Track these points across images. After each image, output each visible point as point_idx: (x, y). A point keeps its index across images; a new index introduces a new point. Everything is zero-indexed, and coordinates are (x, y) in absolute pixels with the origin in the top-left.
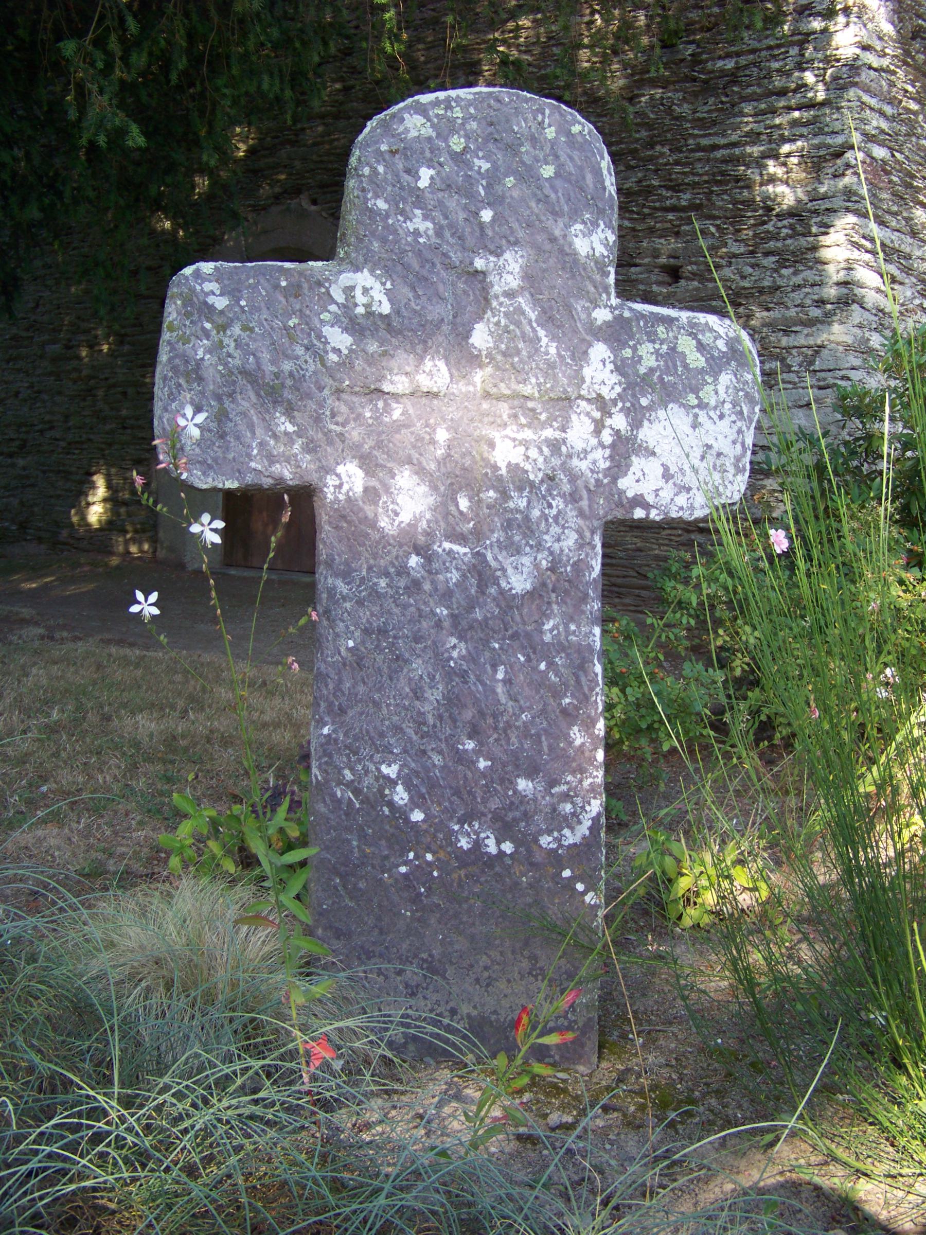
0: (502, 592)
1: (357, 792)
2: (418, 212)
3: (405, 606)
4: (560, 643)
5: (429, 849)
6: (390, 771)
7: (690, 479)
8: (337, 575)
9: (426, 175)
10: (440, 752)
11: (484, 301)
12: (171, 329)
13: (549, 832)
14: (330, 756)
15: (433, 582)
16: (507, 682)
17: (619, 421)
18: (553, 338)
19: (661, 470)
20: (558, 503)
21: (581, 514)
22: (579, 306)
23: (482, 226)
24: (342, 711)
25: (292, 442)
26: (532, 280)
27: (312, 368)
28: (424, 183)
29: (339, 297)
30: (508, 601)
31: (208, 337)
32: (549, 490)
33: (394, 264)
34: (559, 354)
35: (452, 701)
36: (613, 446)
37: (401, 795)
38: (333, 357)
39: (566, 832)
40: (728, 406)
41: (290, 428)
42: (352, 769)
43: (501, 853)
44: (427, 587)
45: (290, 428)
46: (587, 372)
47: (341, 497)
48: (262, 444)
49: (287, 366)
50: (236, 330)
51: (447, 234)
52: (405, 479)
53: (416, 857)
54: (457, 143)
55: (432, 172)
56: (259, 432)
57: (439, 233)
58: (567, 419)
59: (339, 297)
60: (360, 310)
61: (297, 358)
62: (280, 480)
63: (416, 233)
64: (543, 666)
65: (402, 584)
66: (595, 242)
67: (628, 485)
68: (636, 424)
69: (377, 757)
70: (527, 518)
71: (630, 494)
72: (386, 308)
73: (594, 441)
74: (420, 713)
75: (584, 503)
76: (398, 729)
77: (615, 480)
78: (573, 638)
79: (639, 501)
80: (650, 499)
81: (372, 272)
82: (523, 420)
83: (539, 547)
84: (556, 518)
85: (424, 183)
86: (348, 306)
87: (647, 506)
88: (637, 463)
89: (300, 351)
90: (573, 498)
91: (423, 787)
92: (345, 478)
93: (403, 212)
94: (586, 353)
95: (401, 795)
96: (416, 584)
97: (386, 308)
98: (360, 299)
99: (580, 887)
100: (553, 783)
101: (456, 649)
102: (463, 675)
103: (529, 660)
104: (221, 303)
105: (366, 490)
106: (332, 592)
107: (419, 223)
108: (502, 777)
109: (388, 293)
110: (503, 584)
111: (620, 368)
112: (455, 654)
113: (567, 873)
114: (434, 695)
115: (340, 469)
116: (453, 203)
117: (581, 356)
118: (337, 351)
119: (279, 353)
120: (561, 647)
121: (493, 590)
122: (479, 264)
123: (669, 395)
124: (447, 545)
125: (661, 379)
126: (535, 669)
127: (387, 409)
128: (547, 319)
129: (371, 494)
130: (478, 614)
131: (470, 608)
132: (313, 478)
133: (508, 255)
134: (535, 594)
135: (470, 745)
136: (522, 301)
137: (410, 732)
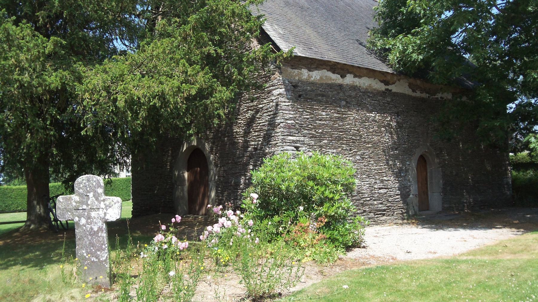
6: (84, 252)
9: (81, 185)
11: (89, 198)
17: (105, 210)
26: (94, 196)
30: (94, 232)
33: (80, 195)
35: (90, 243)
37: (85, 254)
52: (82, 218)
54: (84, 181)
66: (100, 191)
67: (106, 218)
88: (107, 215)
90: (101, 219)
91: (88, 253)
95: (85, 254)
96: (84, 231)
101: (90, 237)
104: (61, 201)
107: (81, 191)
108: (96, 252)
111: (105, 204)
114: (88, 243)
116: (85, 188)
117: (100, 203)
119: (68, 206)
120: (101, 236)
123: (110, 207)
128: (96, 200)
129: (79, 221)
134: (98, 231)
136: (93, 198)
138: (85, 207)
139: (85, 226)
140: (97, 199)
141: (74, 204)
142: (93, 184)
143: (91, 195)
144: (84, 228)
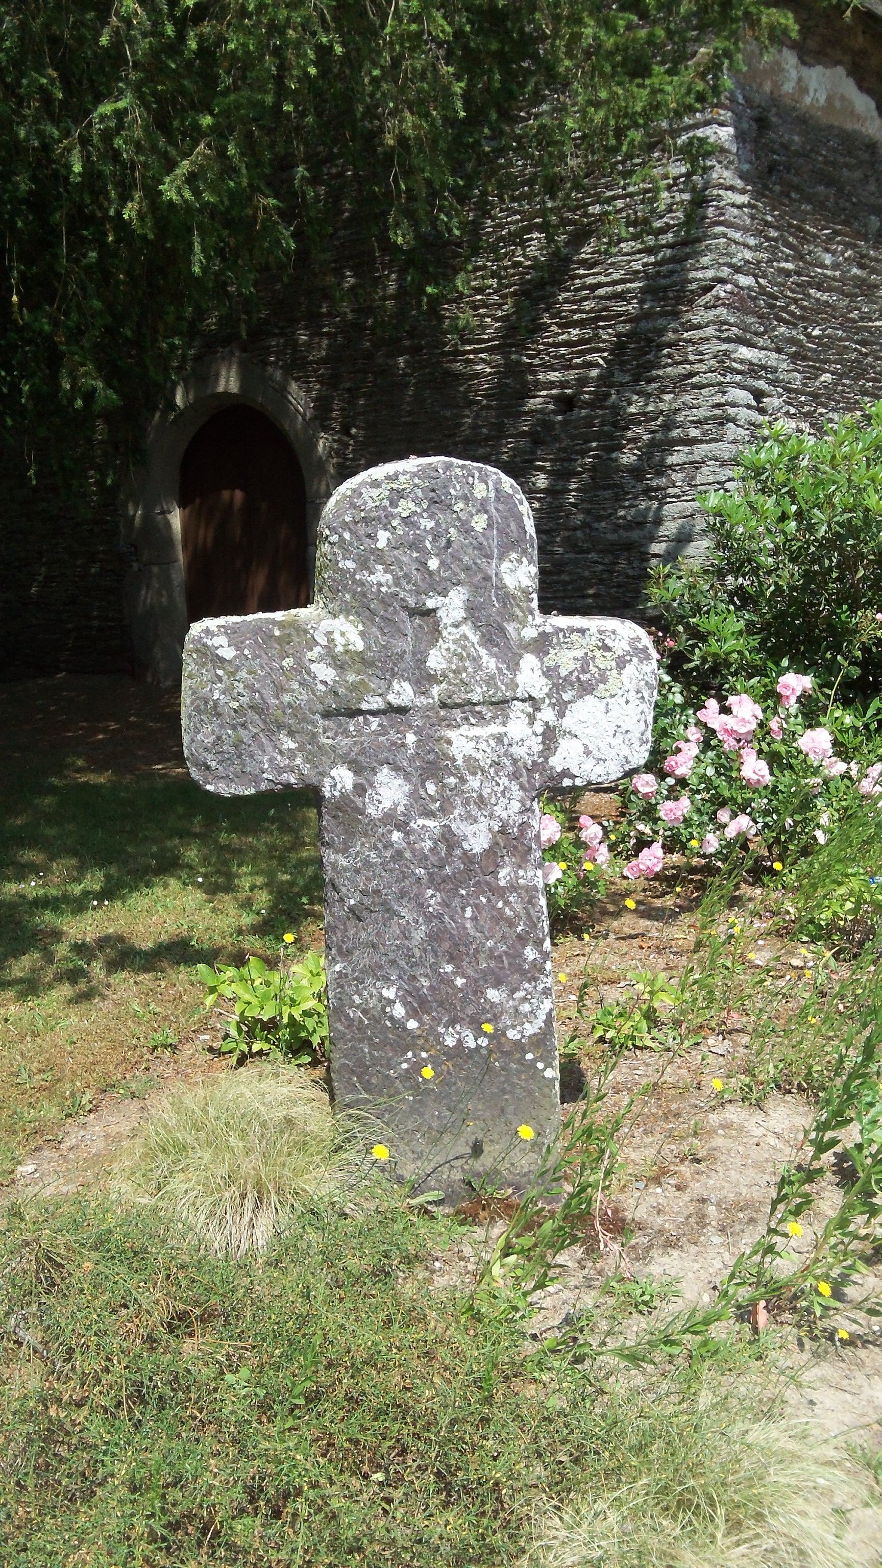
0: (465, 853)
1: (365, 1012)
2: (380, 567)
3: (391, 871)
4: (512, 886)
5: (423, 1049)
6: (390, 993)
7: (606, 753)
8: (337, 852)
9: (383, 538)
10: (427, 976)
11: (436, 633)
12: (190, 677)
13: (514, 1027)
14: (342, 987)
15: (413, 851)
16: (474, 919)
17: (547, 714)
18: (492, 655)
19: (582, 749)
20: (504, 781)
21: (522, 787)
22: (510, 628)
23: (431, 573)
24: (349, 952)
25: (295, 756)
26: (473, 611)
27: (305, 697)
28: (382, 544)
29: (323, 641)
30: (468, 858)
31: (221, 681)
32: (496, 772)
33: (364, 606)
34: (498, 668)
35: (433, 938)
36: (543, 734)
37: (399, 1011)
38: (322, 687)
39: (527, 1025)
40: (632, 693)
41: (293, 745)
42: (360, 995)
43: (479, 1047)
44: (408, 855)
45: (293, 745)
46: (520, 679)
47: (337, 794)
48: (271, 760)
49: (287, 698)
50: (243, 674)
51: (404, 582)
52: (384, 775)
53: (414, 1056)
54: (406, 507)
55: (388, 534)
56: (269, 749)
57: (397, 584)
58: (507, 717)
59: (323, 641)
60: (339, 649)
61: (293, 691)
62: (288, 786)
63: (380, 584)
64: (500, 905)
65: (388, 854)
66: (521, 574)
67: (557, 762)
68: (561, 715)
69: (379, 984)
70: (481, 796)
71: (559, 769)
72: (360, 646)
73: (530, 731)
74: (409, 949)
75: (524, 779)
76: (393, 962)
77: (547, 759)
78: (521, 881)
79: (566, 773)
80: (575, 771)
81: (347, 618)
82: (473, 721)
83: (491, 816)
84: (503, 793)
85: (382, 544)
86: (330, 648)
87: (574, 777)
88: (565, 744)
89: (296, 686)
90: (515, 776)
92: (338, 779)
93: (367, 569)
94: (518, 664)
95: (399, 1011)
96: (399, 854)
97: (360, 646)
98: (339, 640)
99: (540, 1065)
100: (513, 991)
101: (433, 899)
102: (439, 917)
103: (489, 901)
104: (228, 653)
105: (356, 786)
106: (334, 865)
107: (380, 576)
108: (476, 989)
109: (362, 634)
110: (466, 846)
111: (548, 673)
112: (432, 902)
113: (529, 1056)
114: (419, 935)
115: (334, 773)
116: (408, 557)
117: (514, 666)
118: (325, 683)
119: (280, 690)
120: (513, 887)
121: (458, 852)
122: (430, 604)
123: (586, 689)
124: (421, 822)
125: (578, 679)
126: (494, 907)
127: (367, 723)
128: (488, 641)
129: (360, 790)
130: (448, 870)
131: (442, 867)
132: (314, 781)
133: (452, 594)
134: (491, 852)
135: (449, 968)
136: (467, 629)
137: (403, 963)
138: (403, 693)
139: (402, 826)
140: (493, 636)
141: (325, 673)
142: (466, 529)
143: (452, 606)
144: (396, 836)
